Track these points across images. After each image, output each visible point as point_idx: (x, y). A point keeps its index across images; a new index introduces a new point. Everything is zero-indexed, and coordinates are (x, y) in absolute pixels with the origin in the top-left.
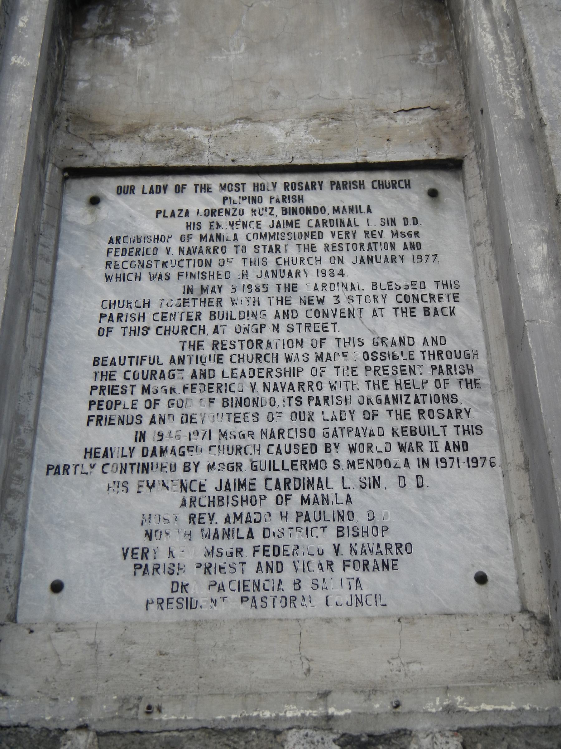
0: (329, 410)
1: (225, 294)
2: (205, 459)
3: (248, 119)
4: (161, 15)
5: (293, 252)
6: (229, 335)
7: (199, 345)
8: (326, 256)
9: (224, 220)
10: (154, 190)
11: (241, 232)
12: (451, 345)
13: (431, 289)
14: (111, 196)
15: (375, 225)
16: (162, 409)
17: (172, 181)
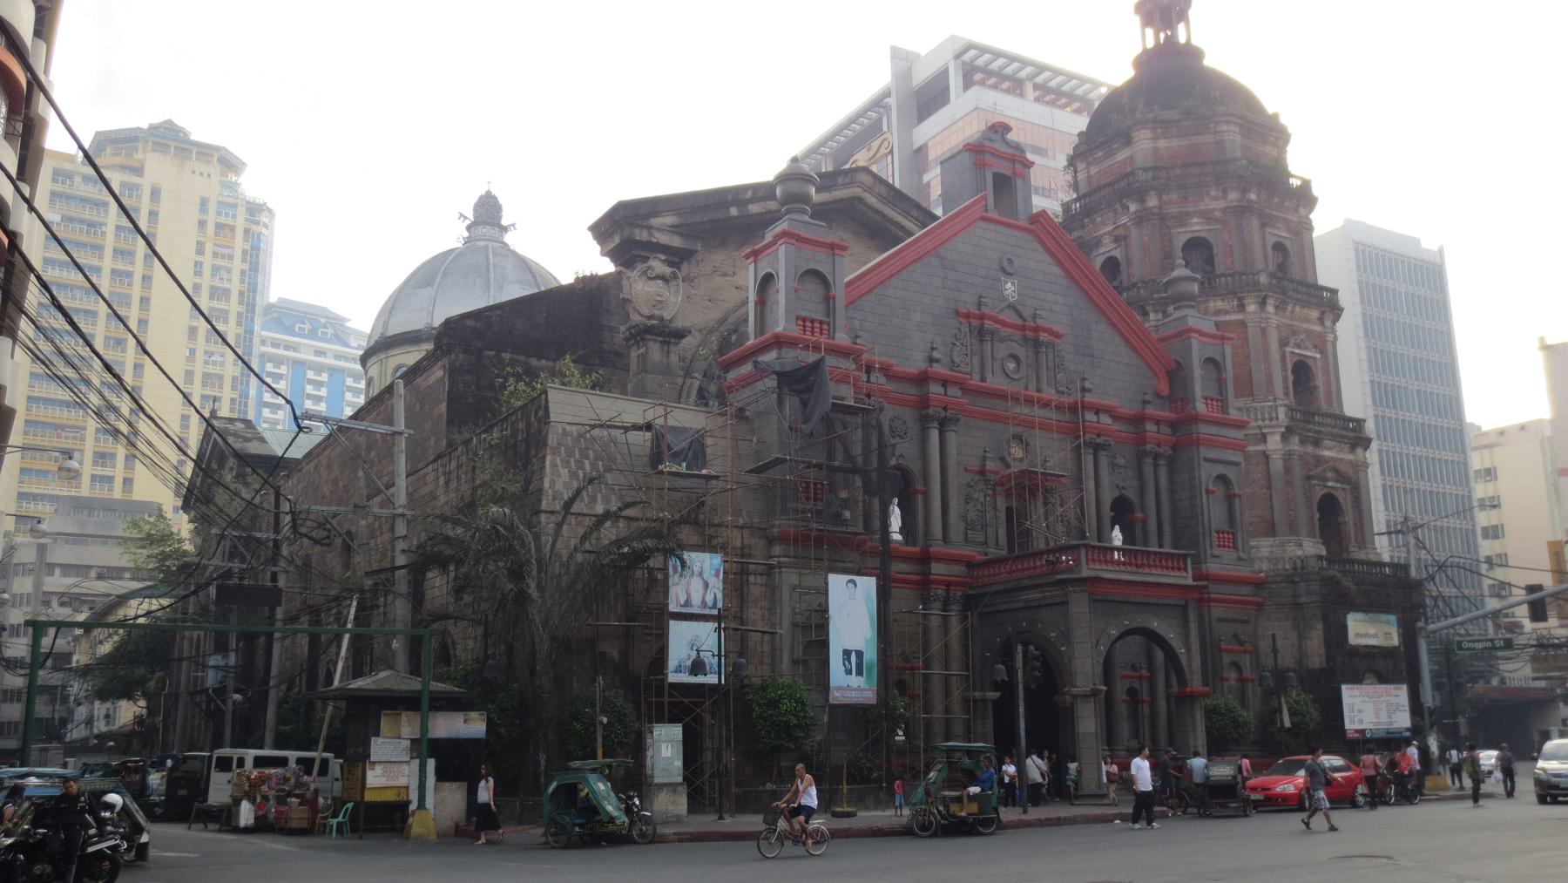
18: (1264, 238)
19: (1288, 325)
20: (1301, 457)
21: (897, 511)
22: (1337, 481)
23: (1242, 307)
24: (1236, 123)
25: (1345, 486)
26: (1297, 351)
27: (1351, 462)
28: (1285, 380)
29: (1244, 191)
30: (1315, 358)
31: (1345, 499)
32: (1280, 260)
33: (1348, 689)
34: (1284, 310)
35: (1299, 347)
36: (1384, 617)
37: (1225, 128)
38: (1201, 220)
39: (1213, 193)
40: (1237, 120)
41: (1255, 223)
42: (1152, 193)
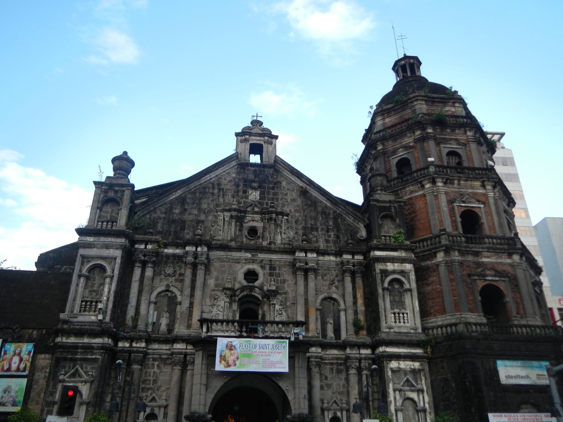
18: (440, 150)
19: (457, 192)
20: (461, 263)
21: (167, 315)
22: (495, 276)
23: (423, 186)
24: (422, 100)
25: (503, 279)
26: (463, 205)
27: (510, 264)
28: (454, 222)
29: (424, 129)
30: (480, 207)
31: (502, 286)
32: (457, 161)
33: (494, 416)
34: (453, 184)
35: (464, 202)
36: (535, 363)
37: (415, 103)
38: (403, 149)
39: (409, 135)
40: (422, 98)
41: (431, 144)
42: (379, 143)
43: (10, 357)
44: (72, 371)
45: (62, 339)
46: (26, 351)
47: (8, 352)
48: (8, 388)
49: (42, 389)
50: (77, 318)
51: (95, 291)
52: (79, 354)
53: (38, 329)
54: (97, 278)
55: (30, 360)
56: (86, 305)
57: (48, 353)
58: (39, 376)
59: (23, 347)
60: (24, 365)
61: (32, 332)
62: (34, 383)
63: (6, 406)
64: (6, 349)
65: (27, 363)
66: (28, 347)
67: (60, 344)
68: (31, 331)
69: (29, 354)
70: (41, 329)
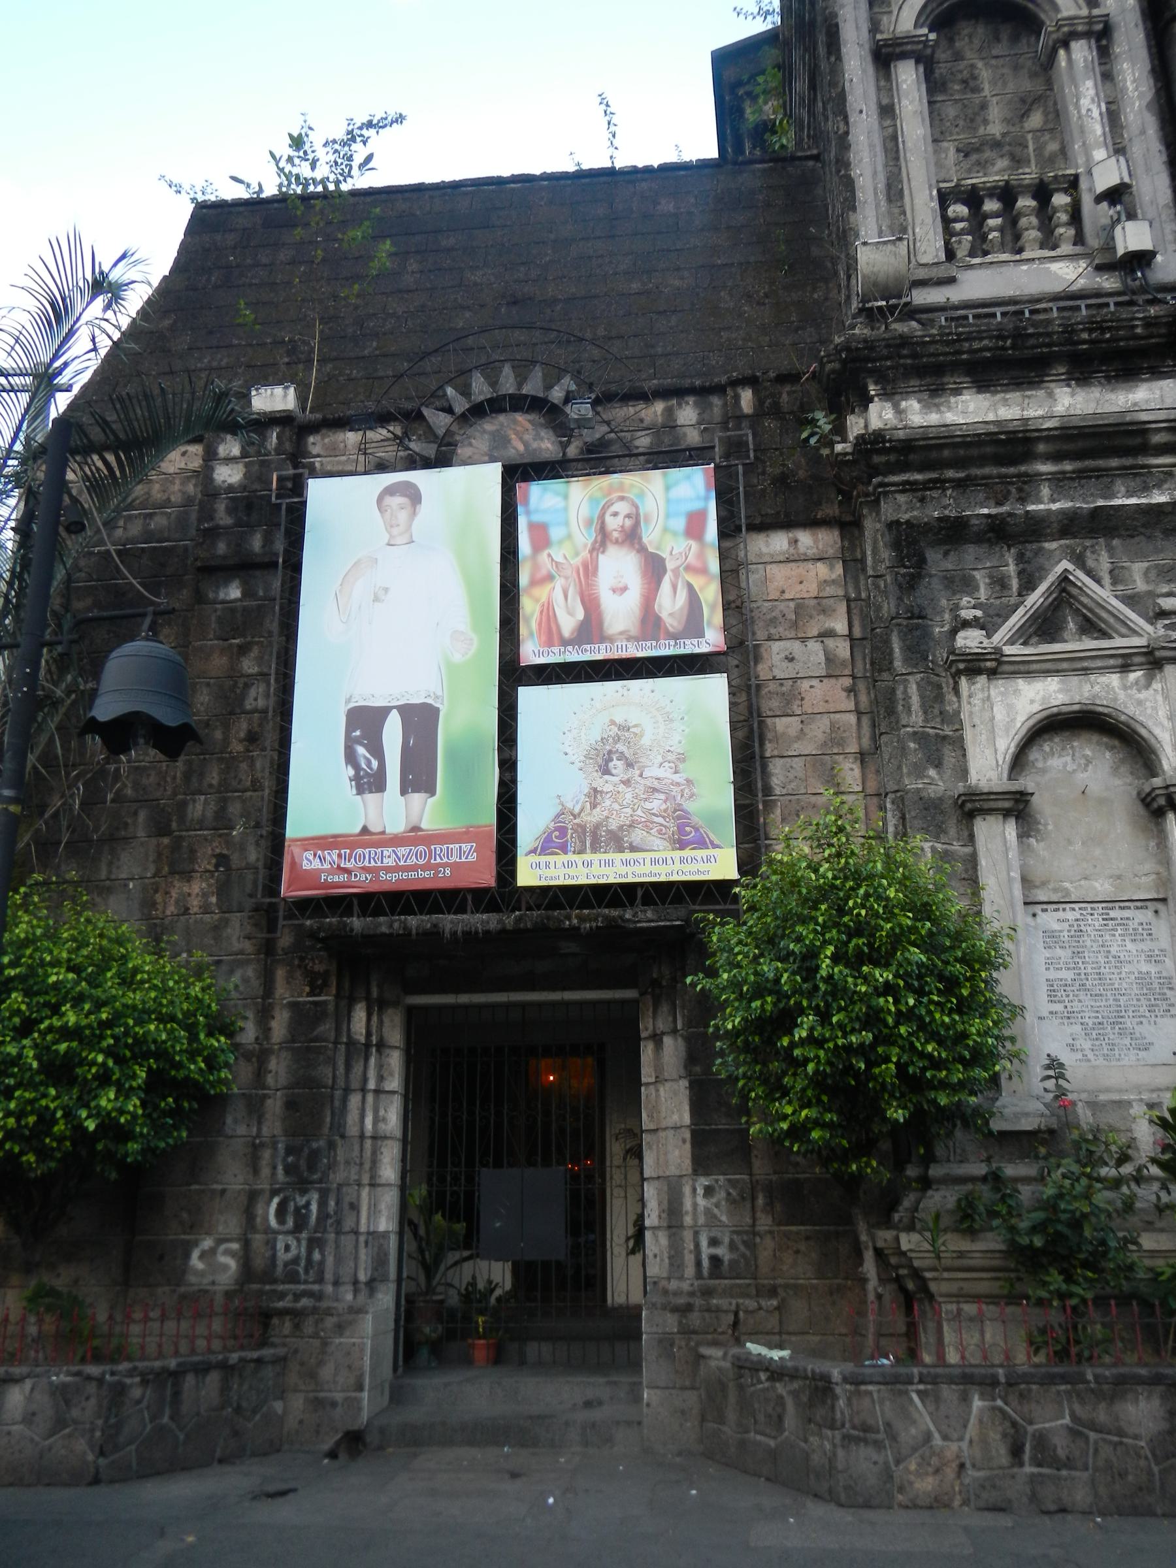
0: (1125, 998)
1: (1086, 954)
2: (1087, 1015)
3: (1085, 878)
4: (1046, 825)
5: (1108, 937)
6: (1089, 971)
7: (1079, 974)
8: (1119, 939)
9: (1082, 923)
10: (1057, 910)
11: (1089, 929)
12: (1164, 974)
13: (1157, 952)
14: (1040, 912)
15: (1136, 926)
16: (1071, 997)
17: (1061, 906)
43: (577, 561)
44: (1035, 599)
45: (899, 412)
46: (668, 516)
47: (555, 533)
48: (617, 739)
49: (835, 739)
50: (951, 281)
51: (996, 145)
52: (1045, 491)
53: (702, 392)
54: (985, 75)
55: (714, 566)
56: (978, 218)
57: (812, 523)
58: (790, 659)
59: (642, 495)
60: (682, 596)
61: (669, 412)
62: (770, 704)
63: (633, 849)
64: (536, 518)
65: (697, 582)
66: (675, 493)
67: (901, 434)
68: (659, 407)
69: (694, 527)
70: (720, 390)
